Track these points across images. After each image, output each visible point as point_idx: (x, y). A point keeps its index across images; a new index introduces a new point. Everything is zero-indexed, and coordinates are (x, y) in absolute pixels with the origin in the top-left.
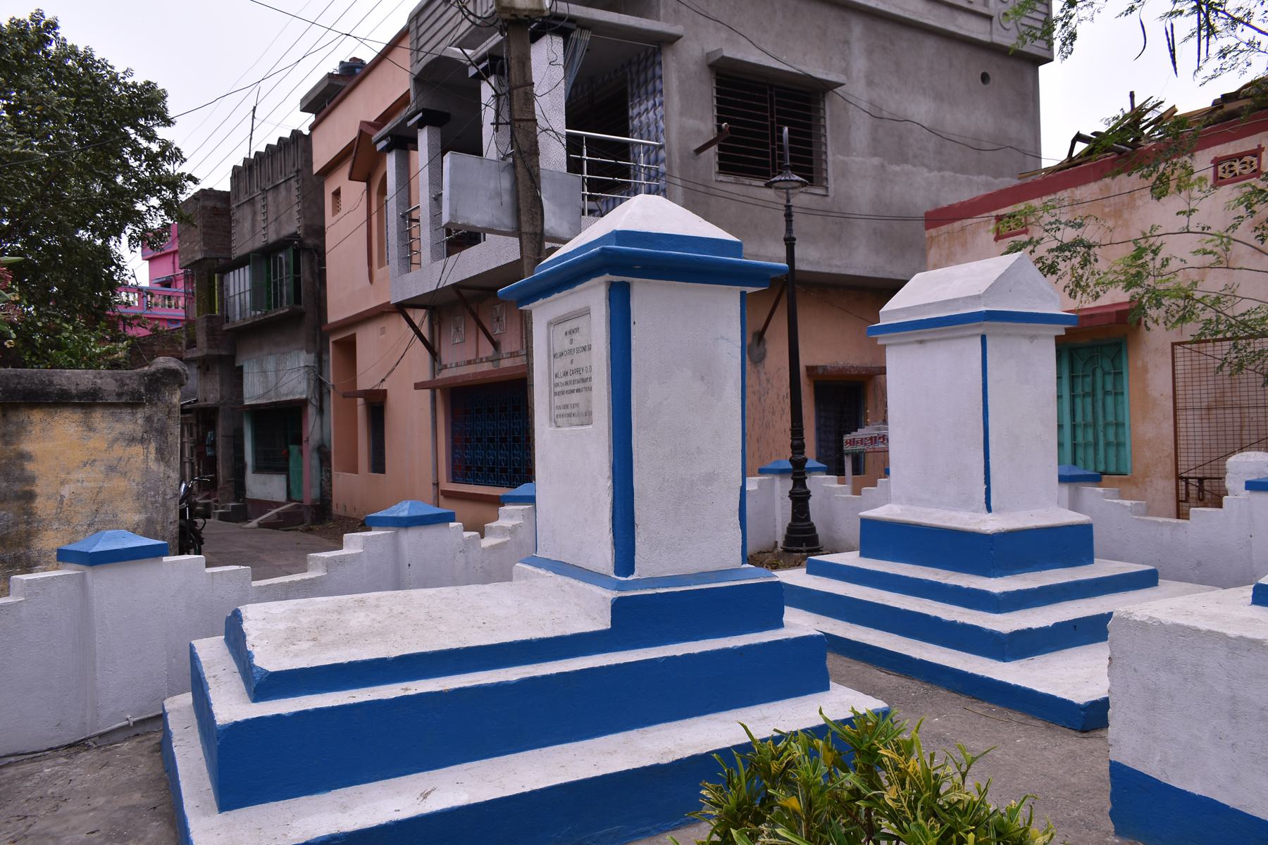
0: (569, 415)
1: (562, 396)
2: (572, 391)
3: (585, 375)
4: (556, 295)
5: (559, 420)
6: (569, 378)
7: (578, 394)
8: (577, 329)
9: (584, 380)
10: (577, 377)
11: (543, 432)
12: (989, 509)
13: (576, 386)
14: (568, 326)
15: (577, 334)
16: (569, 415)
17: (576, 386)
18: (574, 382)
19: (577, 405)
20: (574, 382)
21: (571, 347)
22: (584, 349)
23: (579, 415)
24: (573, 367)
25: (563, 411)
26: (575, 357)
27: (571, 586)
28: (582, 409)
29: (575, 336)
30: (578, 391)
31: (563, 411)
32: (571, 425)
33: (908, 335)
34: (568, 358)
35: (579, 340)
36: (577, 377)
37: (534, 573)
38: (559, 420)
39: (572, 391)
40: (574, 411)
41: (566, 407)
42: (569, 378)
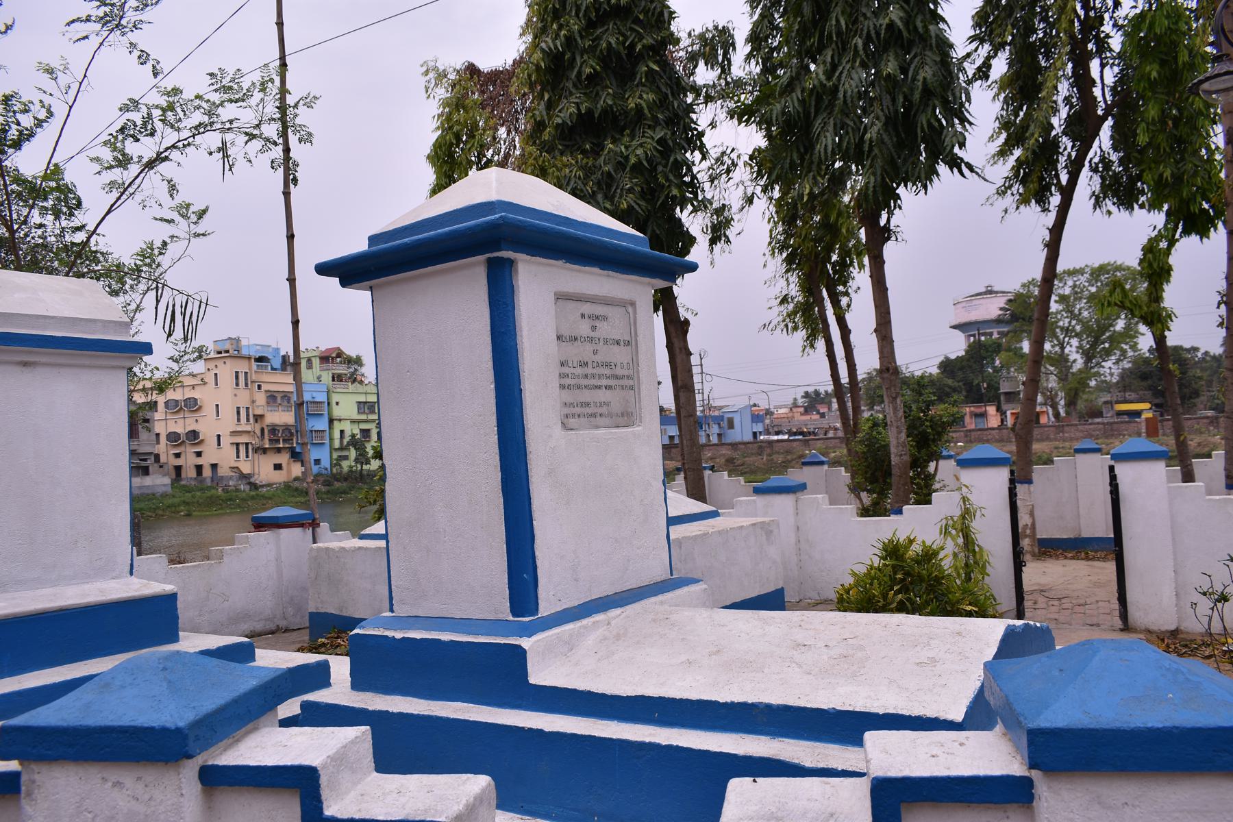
0: (594, 415)
1: (577, 391)
2: (599, 387)
3: (619, 371)
4: (596, 270)
5: (571, 420)
6: (589, 370)
7: (608, 392)
8: (605, 318)
9: (617, 377)
10: (607, 371)
11: (550, 436)
12: (131, 573)
13: (604, 382)
14: (587, 308)
15: (605, 323)
16: (594, 415)
17: (604, 382)
18: (600, 377)
19: (607, 404)
20: (600, 377)
21: (592, 334)
22: (618, 342)
23: (610, 415)
24: (598, 358)
25: (578, 410)
26: (600, 347)
27: (662, 603)
28: (616, 407)
29: (597, 324)
30: (608, 387)
31: (578, 410)
32: (597, 427)
33: (59, 354)
34: (589, 347)
35: (605, 330)
36: (607, 371)
37: (585, 627)
38: (572, 422)
39: (599, 387)
40: (604, 410)
41: (588, 404)
42: (589, 370)
